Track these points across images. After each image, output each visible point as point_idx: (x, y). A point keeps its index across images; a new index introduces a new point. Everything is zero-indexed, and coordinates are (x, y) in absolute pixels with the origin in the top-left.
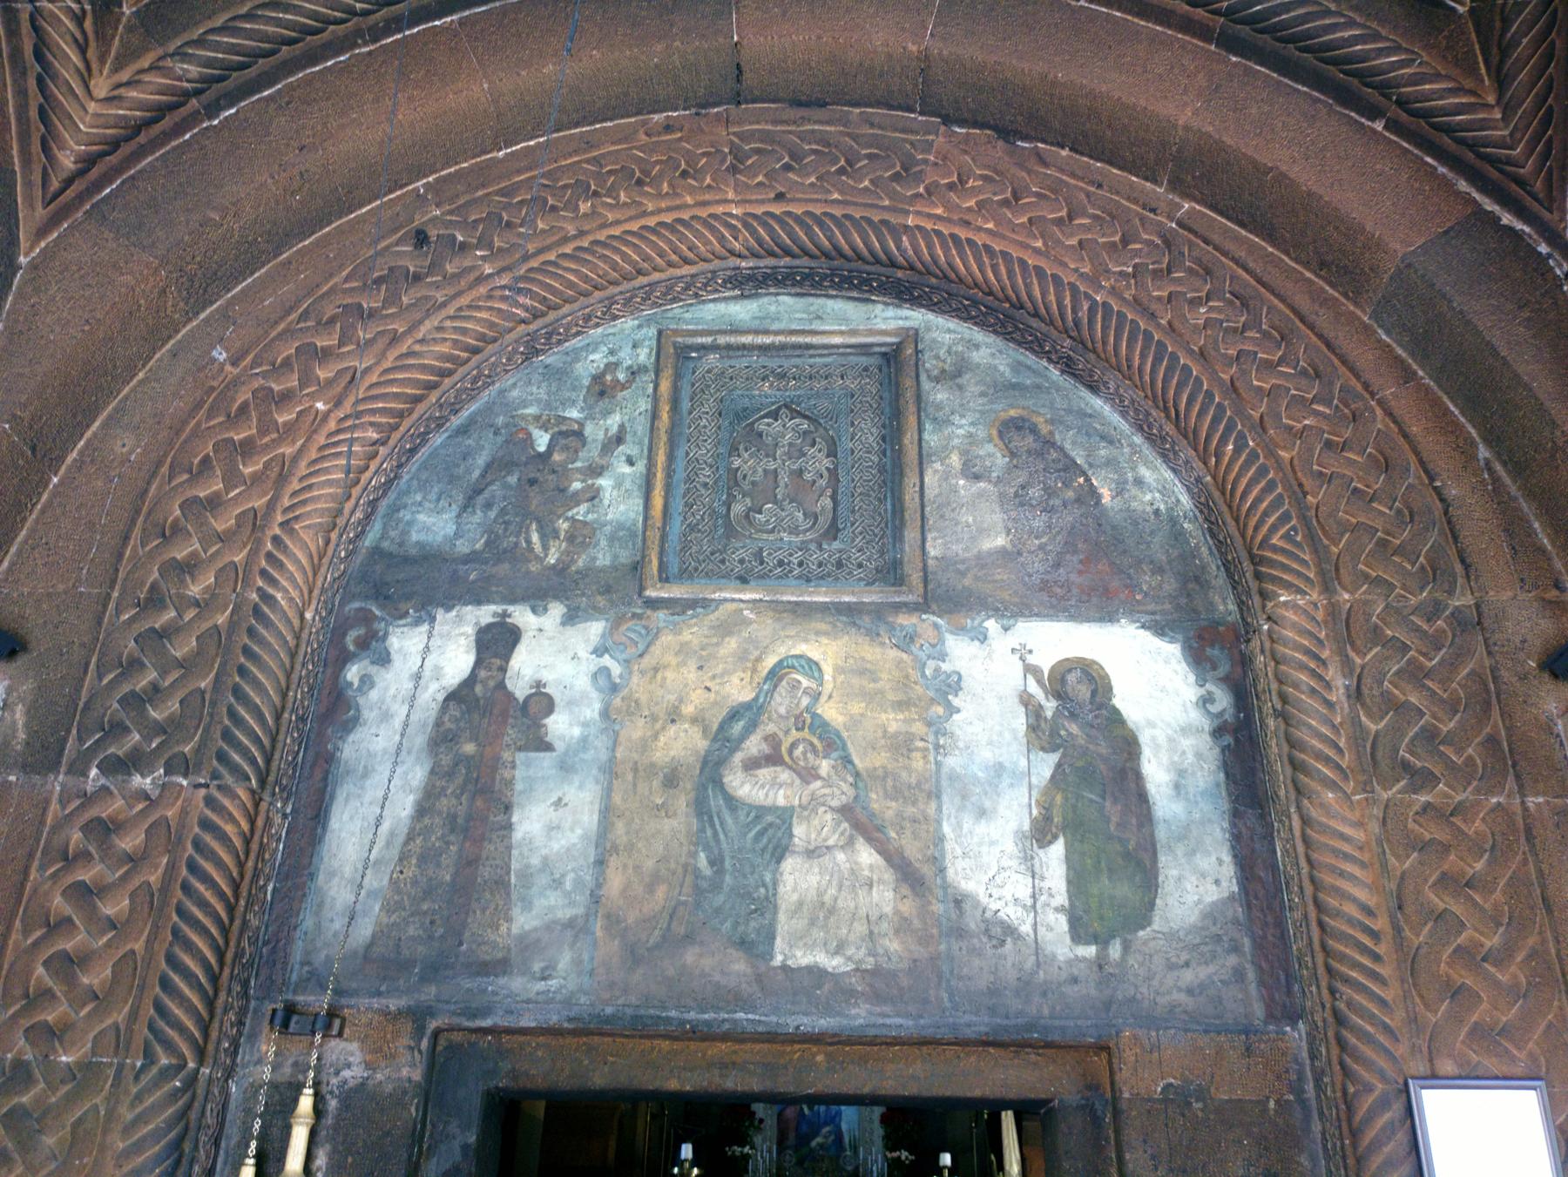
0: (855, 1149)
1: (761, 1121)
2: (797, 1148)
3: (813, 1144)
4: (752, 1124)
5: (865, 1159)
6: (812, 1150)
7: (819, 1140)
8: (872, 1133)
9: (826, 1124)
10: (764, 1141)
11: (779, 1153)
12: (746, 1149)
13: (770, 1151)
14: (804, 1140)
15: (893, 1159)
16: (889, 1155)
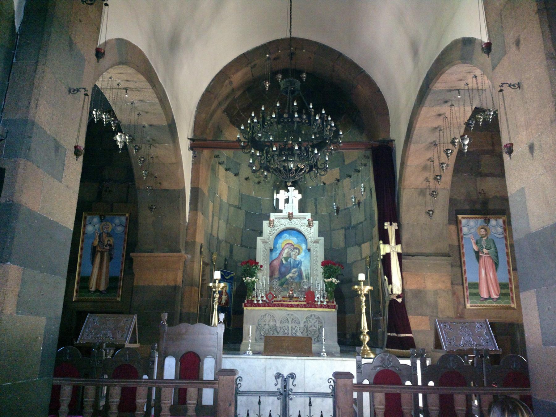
0: (308, 278)
1: (261, 266)
2: (279, 279)
3: (288, 277)
4: (257, 268)
5: (314, 283)
6: (287, 280)
7: (290, 275)
8: (317, 271)
9: (294, 267)
10: (263, 275)
11: (270, 281)
12: (254, 279)
13: (266, 280)
14: (282, 275)
15: (328, 282)
16: (326, 280)
